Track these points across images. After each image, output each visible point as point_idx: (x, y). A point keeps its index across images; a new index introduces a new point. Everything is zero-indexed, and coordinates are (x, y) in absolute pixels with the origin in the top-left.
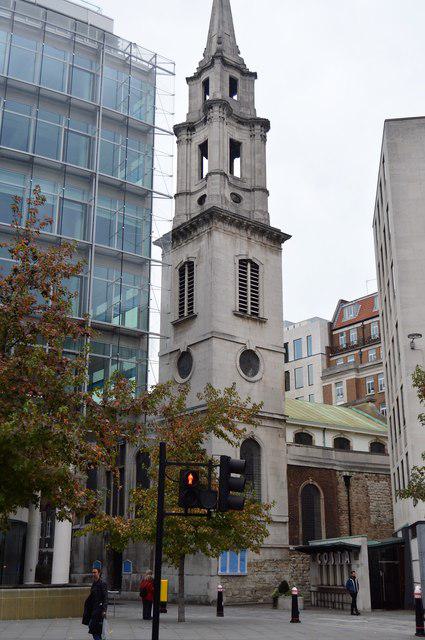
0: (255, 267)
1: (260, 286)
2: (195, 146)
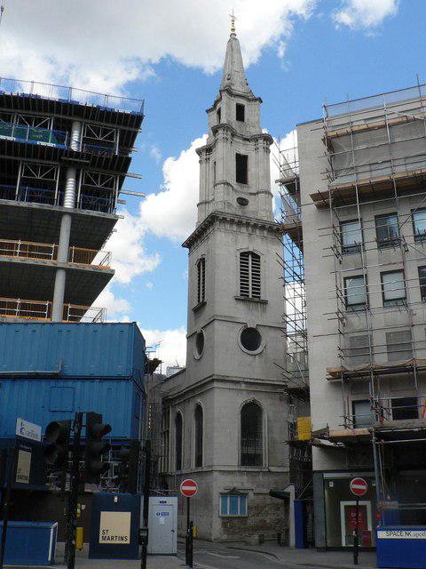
0: (256, 257)
1: (262, 269)
2: (211, 163)
